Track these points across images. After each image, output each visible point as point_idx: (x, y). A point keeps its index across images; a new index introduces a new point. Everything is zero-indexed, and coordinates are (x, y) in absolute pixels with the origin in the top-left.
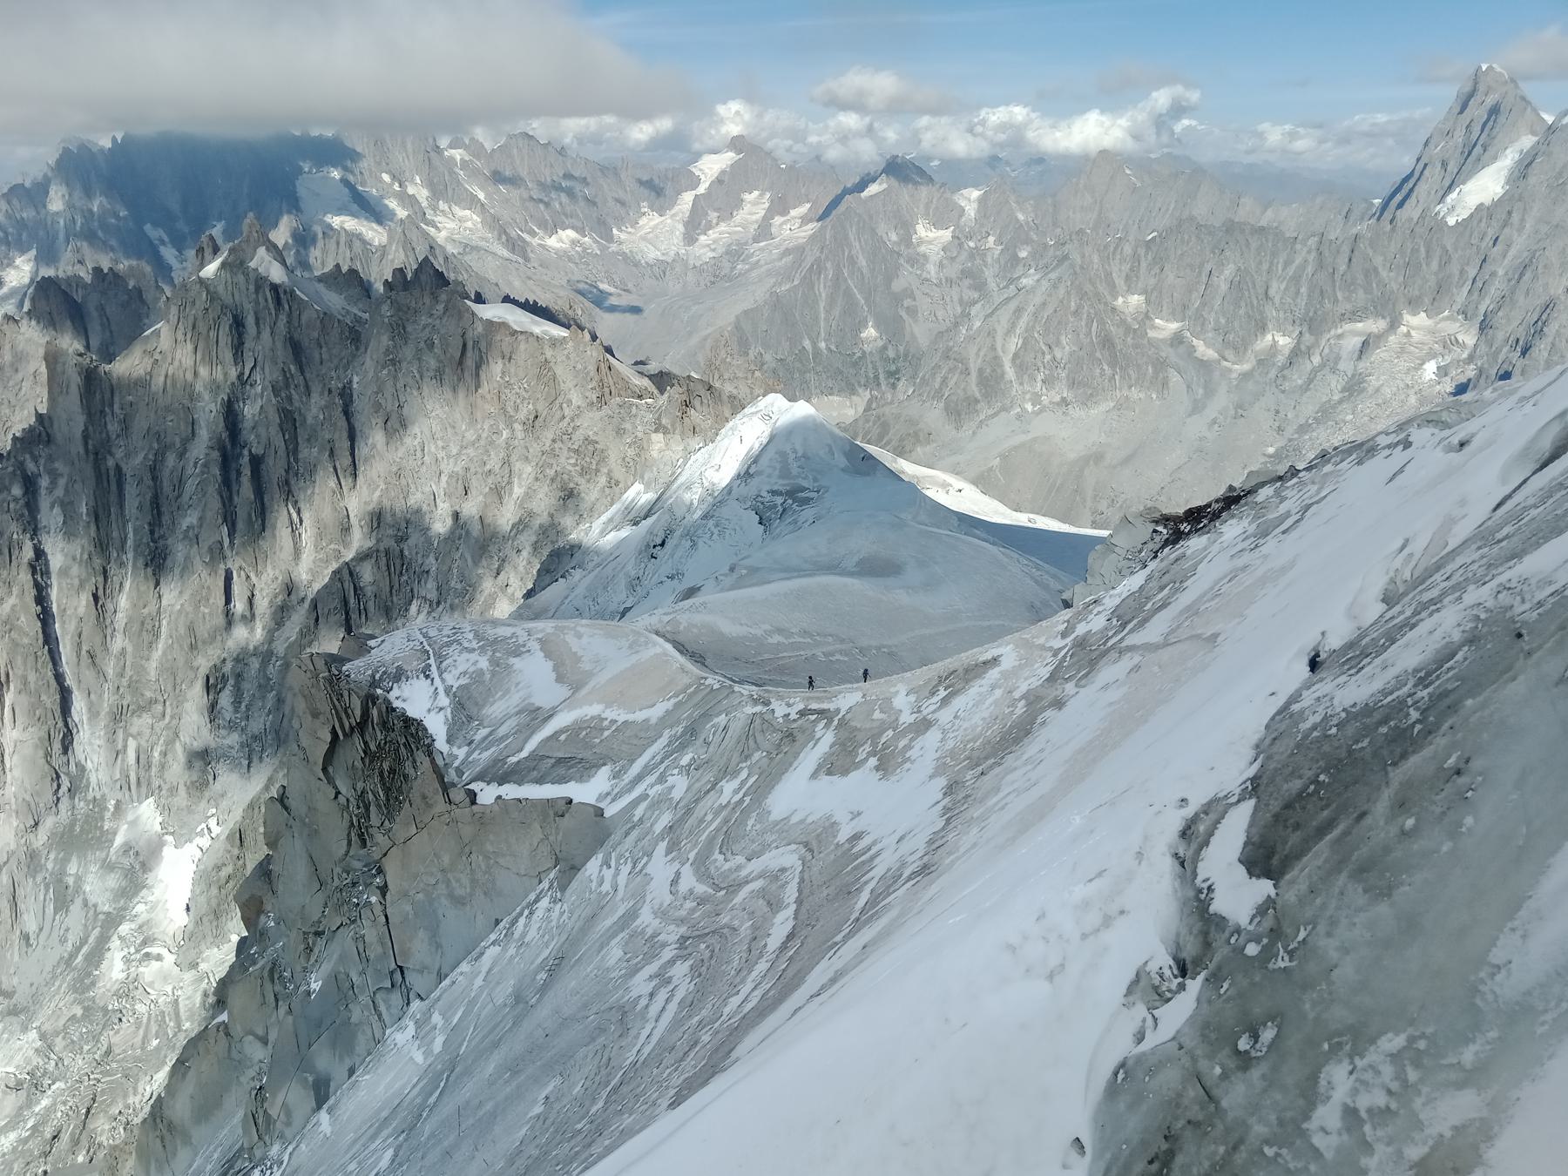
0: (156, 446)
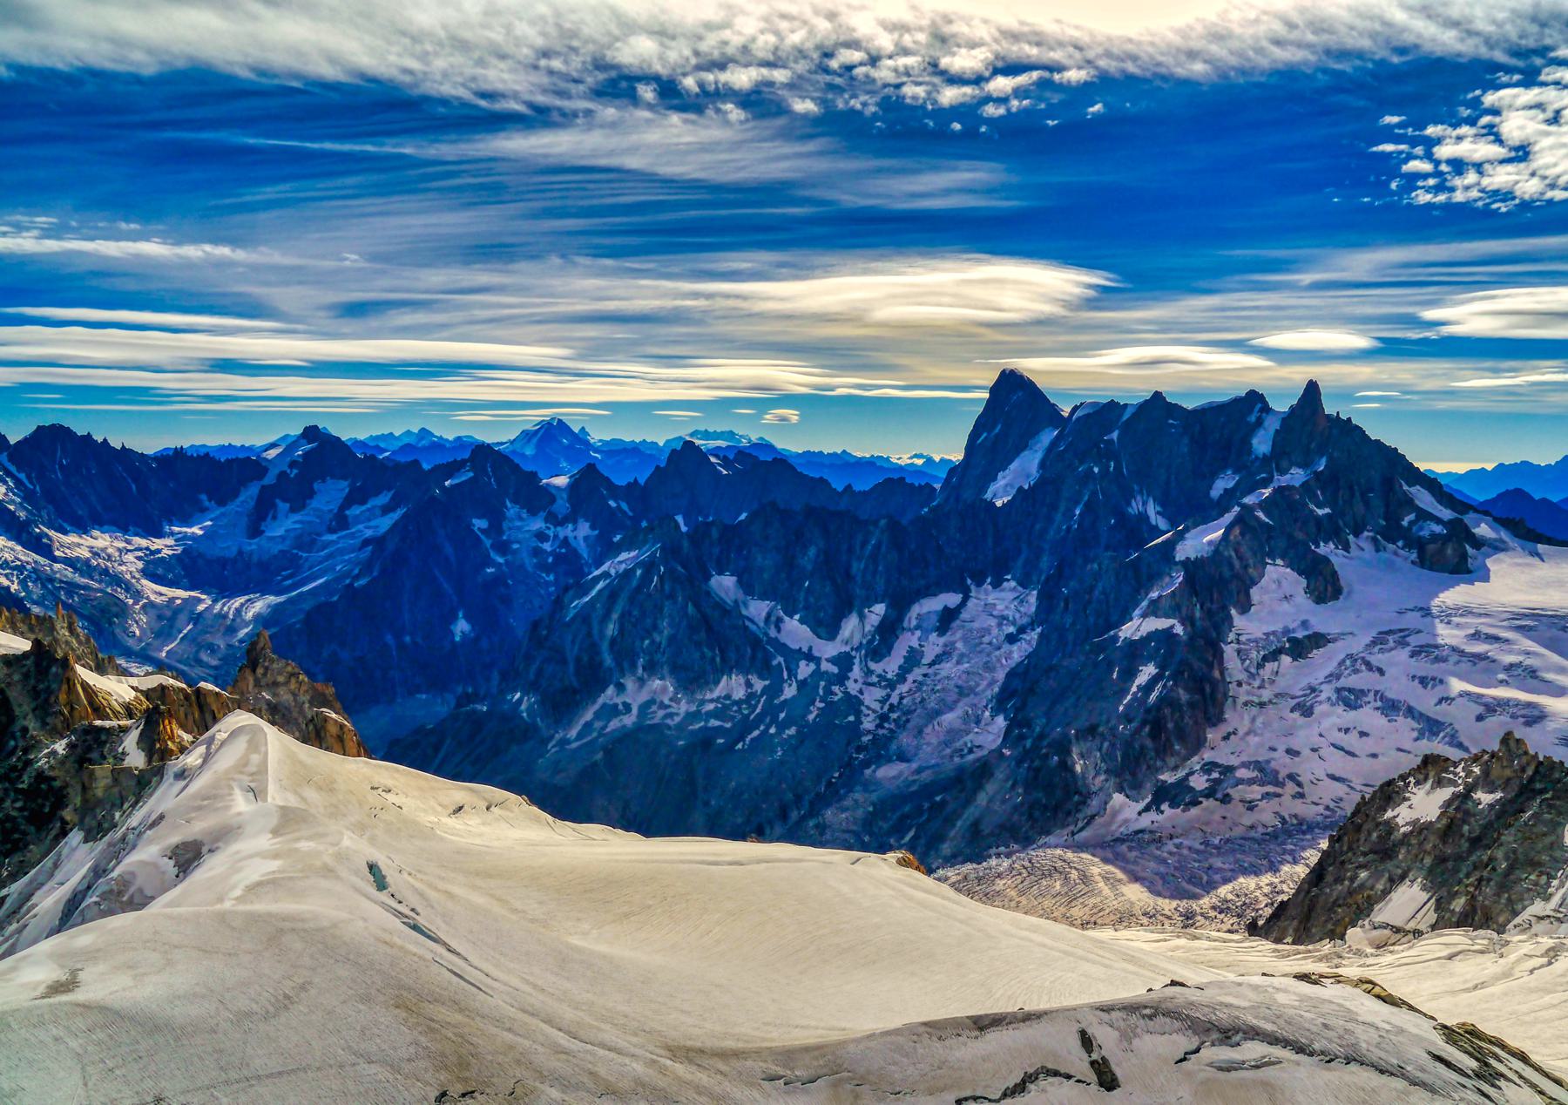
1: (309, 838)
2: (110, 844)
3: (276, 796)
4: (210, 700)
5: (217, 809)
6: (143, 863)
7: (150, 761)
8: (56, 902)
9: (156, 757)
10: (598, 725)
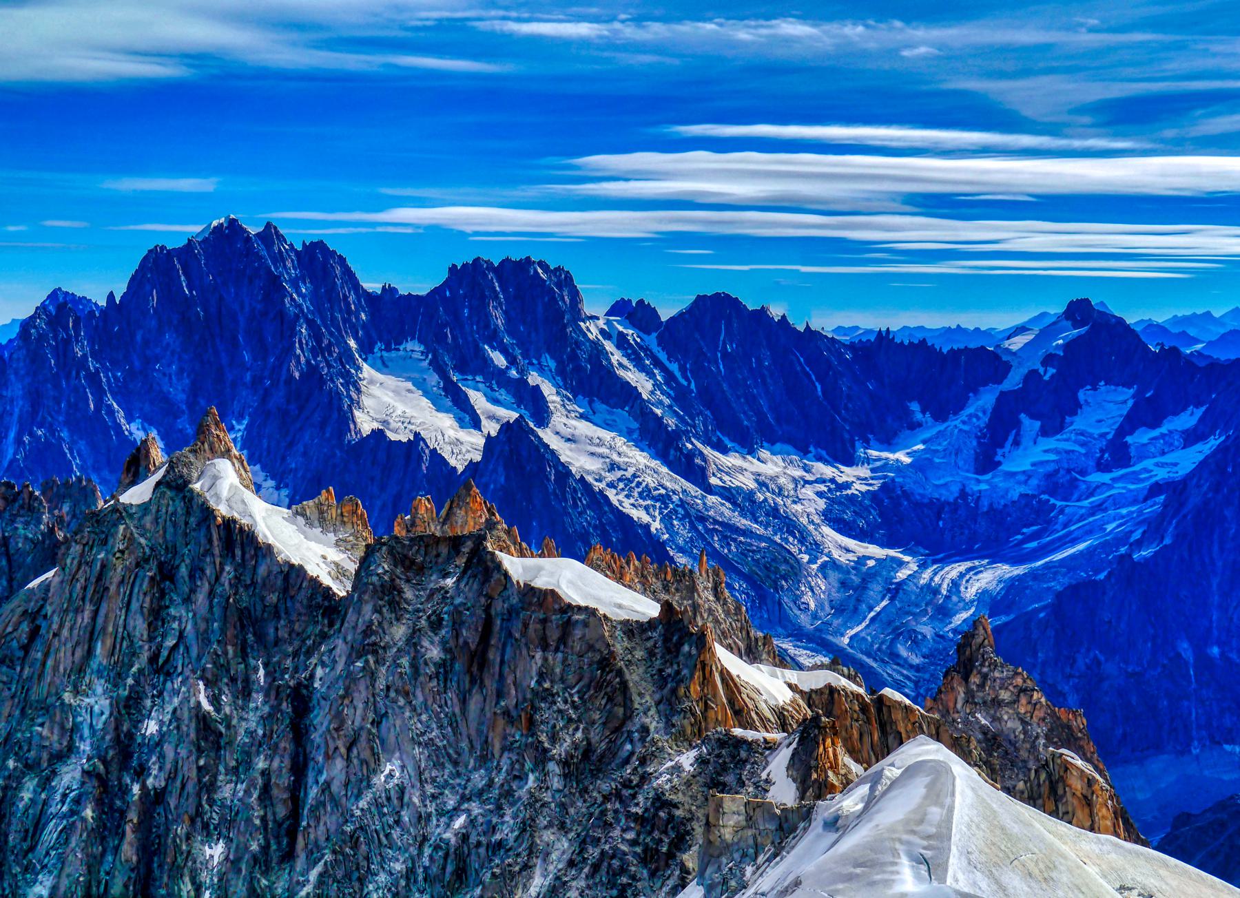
0: (11, 764)
4: (898, 716)
5: (873, 884)
7: (802, 798)
9: (810, 792)
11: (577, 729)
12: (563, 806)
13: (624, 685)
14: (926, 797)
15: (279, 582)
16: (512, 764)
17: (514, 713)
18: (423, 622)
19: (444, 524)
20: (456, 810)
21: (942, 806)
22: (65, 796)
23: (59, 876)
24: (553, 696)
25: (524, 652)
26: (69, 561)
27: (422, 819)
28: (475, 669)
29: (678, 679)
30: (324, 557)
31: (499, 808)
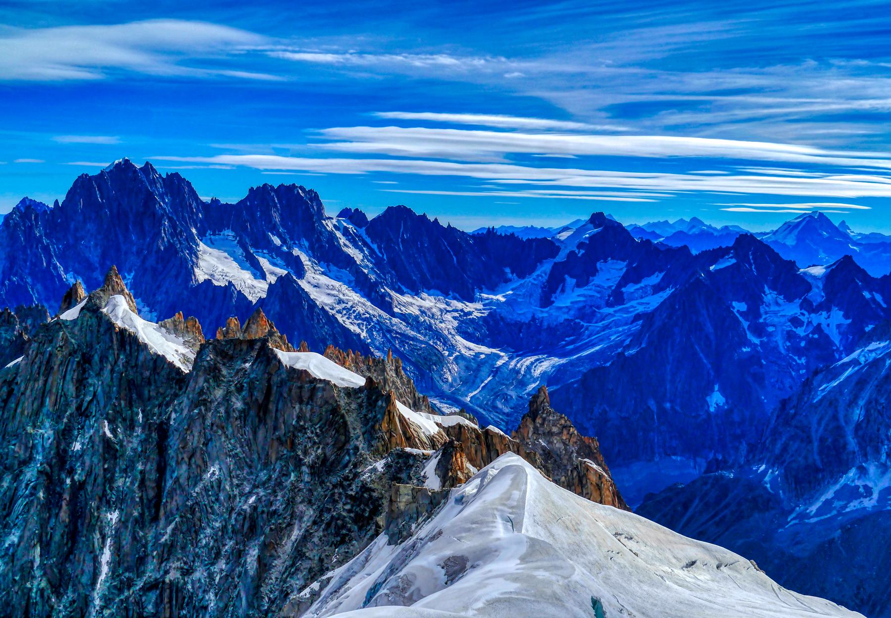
1: (546, 569)
2: (403, 550)
3: (529, 529)
4: (496, 441)
5: (482, 533)
6: (422, 568)
7: (443, 486)
8: (364, 588)
9: (447, 483)
10: (838, 504)
11: (318, 448)
12: (310, 490)
13: (345, 423)
14: (511, 486)
15: (151, 364)
16: (282, 469)
17: (283, 439)
18: (233, 388)
19: (245, 332)
20: (250, 493)
21: (520, 491)
22: (27, 485)
23: (24, 530)
24: (305, 429)
25: (289, 405)
26: (30, 352)
27: (231, 498)
28: (261, 414)
29: (375, 420)
30: (177, 351)
31: (275, 492)
